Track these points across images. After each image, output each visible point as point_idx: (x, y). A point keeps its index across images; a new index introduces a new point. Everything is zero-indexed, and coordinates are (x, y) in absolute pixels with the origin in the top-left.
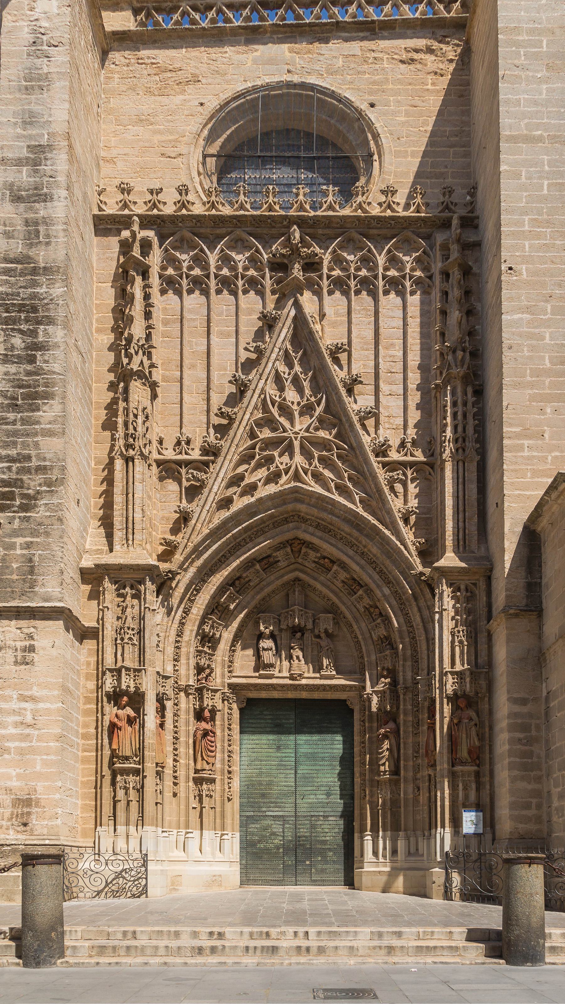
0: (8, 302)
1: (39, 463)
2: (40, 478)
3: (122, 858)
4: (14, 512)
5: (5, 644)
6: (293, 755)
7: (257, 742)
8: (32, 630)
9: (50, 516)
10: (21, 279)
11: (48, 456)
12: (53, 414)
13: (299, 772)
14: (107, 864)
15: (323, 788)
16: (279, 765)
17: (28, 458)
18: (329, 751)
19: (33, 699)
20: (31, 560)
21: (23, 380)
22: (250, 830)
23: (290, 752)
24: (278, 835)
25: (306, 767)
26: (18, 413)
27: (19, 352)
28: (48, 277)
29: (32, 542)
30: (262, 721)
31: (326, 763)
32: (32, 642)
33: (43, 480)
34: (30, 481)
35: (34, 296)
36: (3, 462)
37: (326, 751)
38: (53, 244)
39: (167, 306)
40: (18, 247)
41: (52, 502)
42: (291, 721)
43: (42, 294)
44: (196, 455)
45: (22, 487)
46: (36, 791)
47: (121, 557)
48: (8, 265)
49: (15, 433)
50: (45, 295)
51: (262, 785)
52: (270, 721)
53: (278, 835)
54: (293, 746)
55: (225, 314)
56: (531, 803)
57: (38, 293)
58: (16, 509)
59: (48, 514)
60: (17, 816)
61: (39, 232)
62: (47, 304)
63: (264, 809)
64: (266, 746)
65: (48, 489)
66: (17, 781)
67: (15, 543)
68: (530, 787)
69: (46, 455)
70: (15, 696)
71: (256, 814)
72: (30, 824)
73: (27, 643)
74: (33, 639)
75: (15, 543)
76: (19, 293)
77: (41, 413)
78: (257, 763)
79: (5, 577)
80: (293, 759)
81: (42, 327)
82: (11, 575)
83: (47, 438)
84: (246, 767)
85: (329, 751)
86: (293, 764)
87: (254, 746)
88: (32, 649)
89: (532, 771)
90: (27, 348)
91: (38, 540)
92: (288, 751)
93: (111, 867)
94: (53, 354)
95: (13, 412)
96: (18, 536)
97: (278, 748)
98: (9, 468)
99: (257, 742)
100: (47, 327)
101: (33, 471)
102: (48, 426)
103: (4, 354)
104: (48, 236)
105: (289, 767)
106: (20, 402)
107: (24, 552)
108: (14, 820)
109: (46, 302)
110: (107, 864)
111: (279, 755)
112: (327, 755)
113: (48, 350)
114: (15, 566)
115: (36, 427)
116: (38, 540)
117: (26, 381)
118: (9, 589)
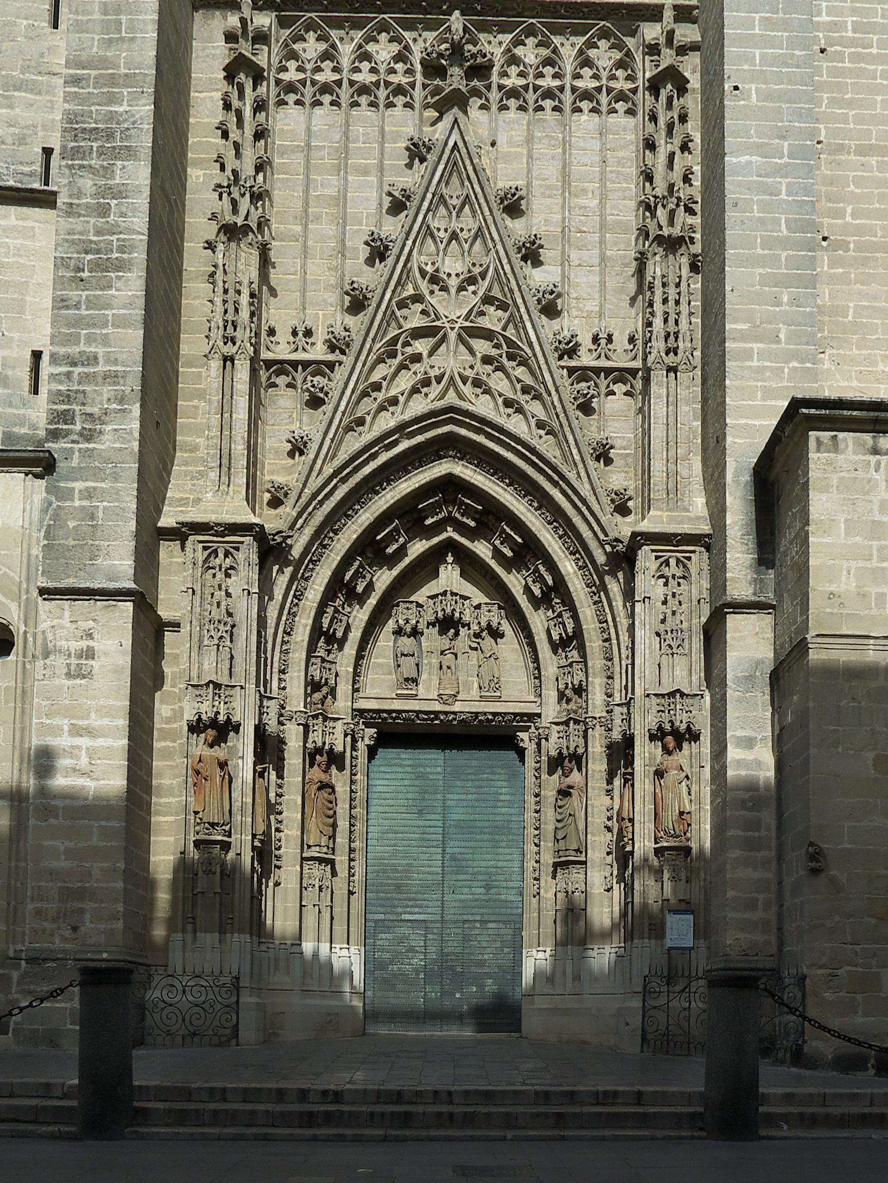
0: (77, 126)
1: (109, 368)
2: (107, 391)
3: (205, 983)
4: (73, 442)
5: (55, 646)
6: (440, 824)
7: (391, 802)
8: (91, 624)
9: (120, 449)
10: (95, 91)
11: (121, 357)
12: (130, 293)
13: (448, 850)
14: (184, 992)
15: (480, 877)
16: (421, 839)
17: (93, 360)
18: (491, 817)
19: (89, 732)
20: (92, 517)
21: (91, 242)
22: (380, 943)
23: (435, 820)
24: (418, 952)
25: (457, 843)
26: (83, 290)
27: (89, 200)
28: (130, 90)
29: (95, 488)
30: (399, 769)
31: (486, 837)
32: (91, 643)
33: (113, 393)
34: (95, 395)
35: (112, 117)
36: (61, 365)
37: (486, 818)
38: (139, 42)
39: (285, 128)
40: (92, 45)
41: (123, 427)
42: (439, 769)
43: (121, 115)
44: (318, 352)
45: (84, 404)
46: (91, 876)
47: (213, 512)
48: (78, 72)
49: (78, 322)
50: (125, 116)
51: (396, 871)
52: (409, 769)
53: (418, 952)
54: (440, 810)
55: (361, 139)
56: (757, 900)
57: (116, 112)
58: (75, 437)
59: (117, 445)
60: (65, 915)
61: (121, 23)
62: (128, 129)
63: (399, 910)
64: (403, 810)
65: (119, 407)
66: (66, 860)
67: (74, 489)
68: (756, 875)
69: (118, 356)
70: (66, 728)
71: (389, 917)
72: (82, 929)
73: (84, 644)
74: (92, 639)
75: (74, 489)
76: (91, 112)
77: (113, 292)
78: (390, 835)
79: (57, 542)
80: (440, 830)
81: (119, 163)
82: (66, 539)
83: (119, 330)
84: (375, 842)
85: (491, 817)
86: (440, 837)
87: (387, 809)
88: (90, 654)
89: (759, 851)
90: (97, 195)
91: (103, 485)
92: (433, 817)
93: (190, 998)
94: (132, 203)
95: (77, 289)
96: (76, 480)
97: (420, 812)
98: (68, 375)
99: (391, 802)
100: (126, 163)
101: (100, 380)
102: (122, 312)
103: (67, 204)
104: (131, 29)
105: (435, 843)
106: (86, 274)
107: (85, 503)
108: (61, 920)
109: (126, 126)
110: (184, 992)
111: (421, 823)
112: (487, 824)
113: (126, 197)
114: (71, 524)
115: (106, 312)
116: (103, 485)
117: (95, 243)
118: (62, 561)
